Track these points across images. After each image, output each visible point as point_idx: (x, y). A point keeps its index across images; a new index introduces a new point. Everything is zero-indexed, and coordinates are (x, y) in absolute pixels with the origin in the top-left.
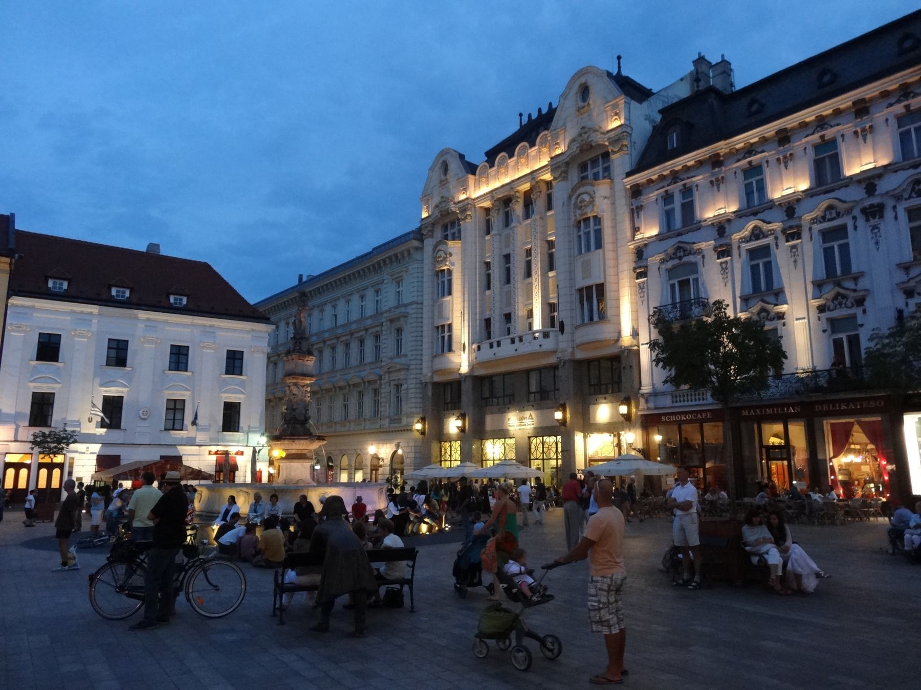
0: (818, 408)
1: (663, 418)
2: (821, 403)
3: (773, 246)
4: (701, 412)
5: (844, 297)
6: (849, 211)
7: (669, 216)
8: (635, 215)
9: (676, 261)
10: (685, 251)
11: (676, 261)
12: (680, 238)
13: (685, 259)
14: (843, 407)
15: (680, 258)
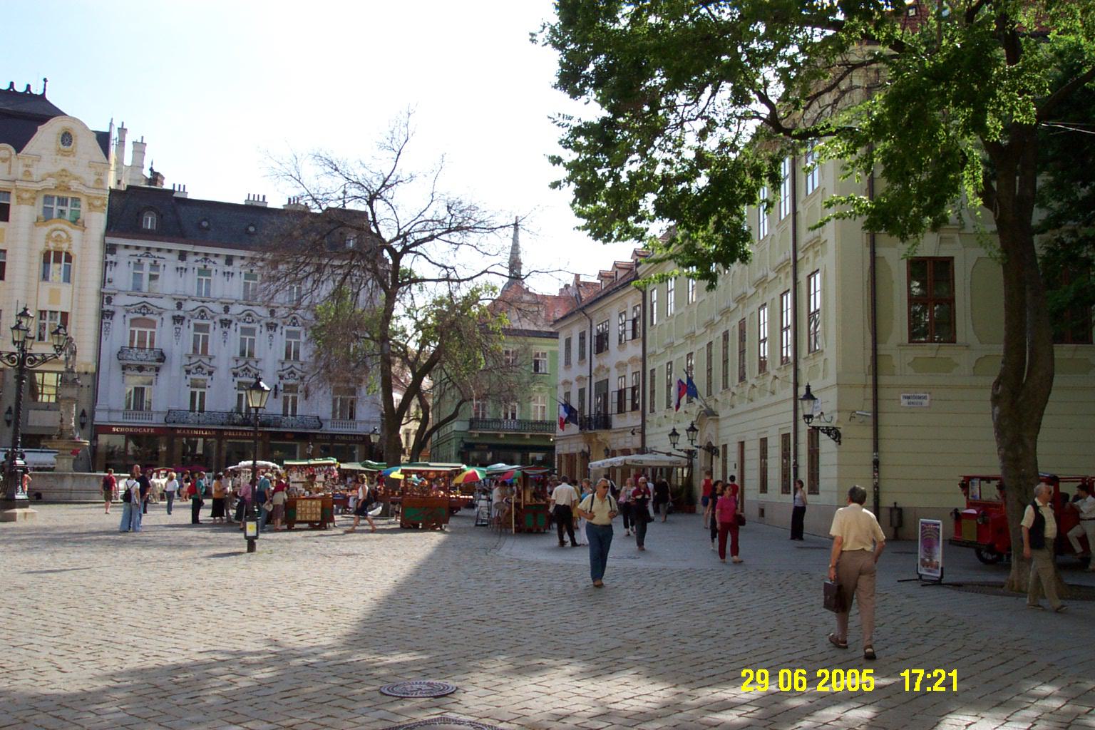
0: (225, 434)
1: (114, 429)
2: (228, 430)
3: (211, 327)
4: (146, 428)
5: (249, 371)
6: (259, 322)
7: (138, 277)
8: (108, 268)
9: (140, 316)
10: (148, 310)
11: (140, 316)
12: (145, 299)
13: (147, 316)
14: (240, 434)
15: (144, 314)
